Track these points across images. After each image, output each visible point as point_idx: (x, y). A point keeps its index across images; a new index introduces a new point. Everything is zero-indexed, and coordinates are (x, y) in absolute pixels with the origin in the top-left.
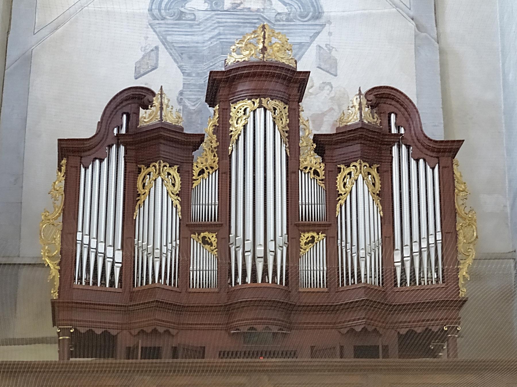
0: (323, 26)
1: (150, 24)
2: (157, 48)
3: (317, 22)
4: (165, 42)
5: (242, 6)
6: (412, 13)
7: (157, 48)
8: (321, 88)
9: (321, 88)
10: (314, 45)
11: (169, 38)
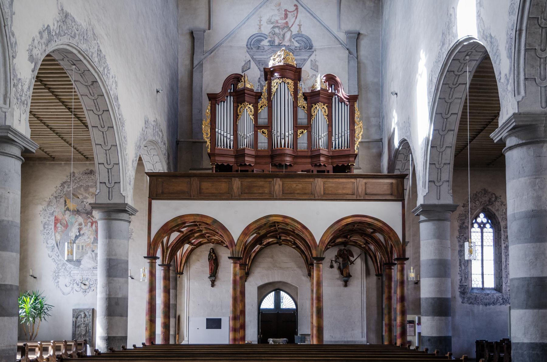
0: (313, 52)
1: (247, 51)
2: (250, 61)
3: (311, 50)
4: (253, 58)
5: (282, 44)
6: (347, 47)
7: (250, 61)
8: (312, 77)
9: (312, 77)
10: (309, 60)
11: (254, 57)
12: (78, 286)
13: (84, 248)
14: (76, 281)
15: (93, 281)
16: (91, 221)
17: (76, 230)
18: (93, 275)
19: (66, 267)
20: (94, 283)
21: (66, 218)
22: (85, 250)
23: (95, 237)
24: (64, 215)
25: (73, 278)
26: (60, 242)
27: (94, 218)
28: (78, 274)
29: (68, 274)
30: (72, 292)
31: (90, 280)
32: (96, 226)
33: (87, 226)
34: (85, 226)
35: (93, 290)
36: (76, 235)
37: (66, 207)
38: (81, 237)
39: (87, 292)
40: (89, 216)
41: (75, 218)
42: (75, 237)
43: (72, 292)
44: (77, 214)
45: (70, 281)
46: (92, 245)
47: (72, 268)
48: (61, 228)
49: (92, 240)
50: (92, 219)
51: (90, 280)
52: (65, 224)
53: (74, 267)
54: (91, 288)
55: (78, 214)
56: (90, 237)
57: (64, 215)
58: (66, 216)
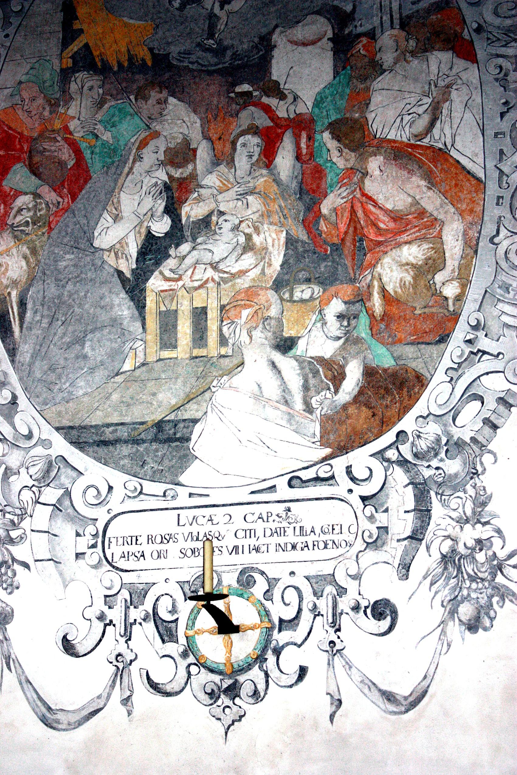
12: (172, 648)
13: (213, 325)
14: (148, 605)
15: (291, 596)
16: (263, 121)
17: (148, 203)
18: (291, 538)
19: (68, 493)
20: (306, 616)
21: (72, 125)
22: (223, 341)
23: (303, 235)
24: (54, 105)
25: (128, 578)
26: (22, 304)
27: (282, 96)
28: (166, 539)
29: (83, 544)
30: (117, 695)
31: (272, 583)
32: (298, 157)
33: (231, 163)
34: (216, 161)
35: (303, 671)
36: (150, 236)
37: (75, 47)
38: (185, 248)
39: (246, 689)
40: (246, 87)
41: (138, 113)
42: (142, 254)
43: (117, 695)
44: (152, 84)
45: (100, 606)
46: (272, 295)
47: (118, 493)
48: (36, 195)
49: (277, 260)
50: (267, 109)
51: (272, 583)
52: (62, 164)
53: (134, 483)
54: (277, 652)
55: (162, 86)
56: (257, 240)
57: (54, 105)
58: (72, 112)
